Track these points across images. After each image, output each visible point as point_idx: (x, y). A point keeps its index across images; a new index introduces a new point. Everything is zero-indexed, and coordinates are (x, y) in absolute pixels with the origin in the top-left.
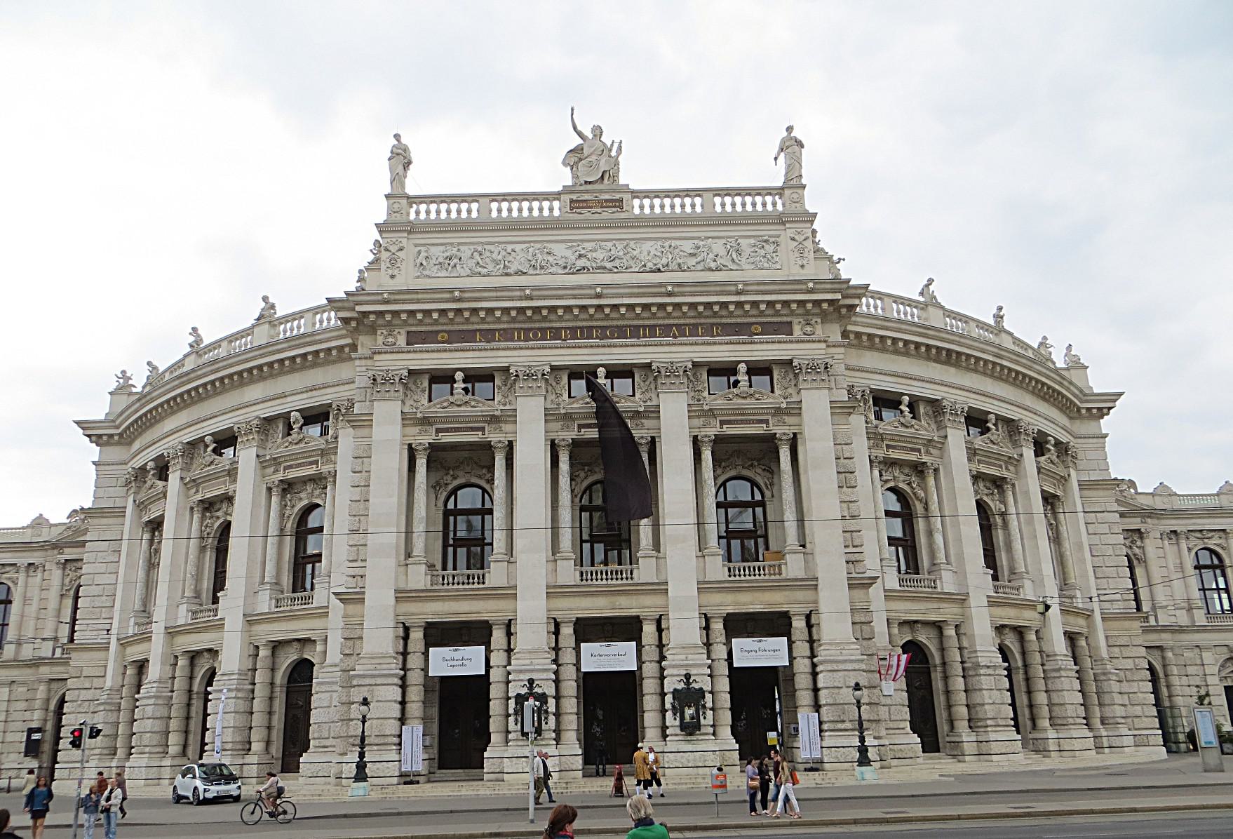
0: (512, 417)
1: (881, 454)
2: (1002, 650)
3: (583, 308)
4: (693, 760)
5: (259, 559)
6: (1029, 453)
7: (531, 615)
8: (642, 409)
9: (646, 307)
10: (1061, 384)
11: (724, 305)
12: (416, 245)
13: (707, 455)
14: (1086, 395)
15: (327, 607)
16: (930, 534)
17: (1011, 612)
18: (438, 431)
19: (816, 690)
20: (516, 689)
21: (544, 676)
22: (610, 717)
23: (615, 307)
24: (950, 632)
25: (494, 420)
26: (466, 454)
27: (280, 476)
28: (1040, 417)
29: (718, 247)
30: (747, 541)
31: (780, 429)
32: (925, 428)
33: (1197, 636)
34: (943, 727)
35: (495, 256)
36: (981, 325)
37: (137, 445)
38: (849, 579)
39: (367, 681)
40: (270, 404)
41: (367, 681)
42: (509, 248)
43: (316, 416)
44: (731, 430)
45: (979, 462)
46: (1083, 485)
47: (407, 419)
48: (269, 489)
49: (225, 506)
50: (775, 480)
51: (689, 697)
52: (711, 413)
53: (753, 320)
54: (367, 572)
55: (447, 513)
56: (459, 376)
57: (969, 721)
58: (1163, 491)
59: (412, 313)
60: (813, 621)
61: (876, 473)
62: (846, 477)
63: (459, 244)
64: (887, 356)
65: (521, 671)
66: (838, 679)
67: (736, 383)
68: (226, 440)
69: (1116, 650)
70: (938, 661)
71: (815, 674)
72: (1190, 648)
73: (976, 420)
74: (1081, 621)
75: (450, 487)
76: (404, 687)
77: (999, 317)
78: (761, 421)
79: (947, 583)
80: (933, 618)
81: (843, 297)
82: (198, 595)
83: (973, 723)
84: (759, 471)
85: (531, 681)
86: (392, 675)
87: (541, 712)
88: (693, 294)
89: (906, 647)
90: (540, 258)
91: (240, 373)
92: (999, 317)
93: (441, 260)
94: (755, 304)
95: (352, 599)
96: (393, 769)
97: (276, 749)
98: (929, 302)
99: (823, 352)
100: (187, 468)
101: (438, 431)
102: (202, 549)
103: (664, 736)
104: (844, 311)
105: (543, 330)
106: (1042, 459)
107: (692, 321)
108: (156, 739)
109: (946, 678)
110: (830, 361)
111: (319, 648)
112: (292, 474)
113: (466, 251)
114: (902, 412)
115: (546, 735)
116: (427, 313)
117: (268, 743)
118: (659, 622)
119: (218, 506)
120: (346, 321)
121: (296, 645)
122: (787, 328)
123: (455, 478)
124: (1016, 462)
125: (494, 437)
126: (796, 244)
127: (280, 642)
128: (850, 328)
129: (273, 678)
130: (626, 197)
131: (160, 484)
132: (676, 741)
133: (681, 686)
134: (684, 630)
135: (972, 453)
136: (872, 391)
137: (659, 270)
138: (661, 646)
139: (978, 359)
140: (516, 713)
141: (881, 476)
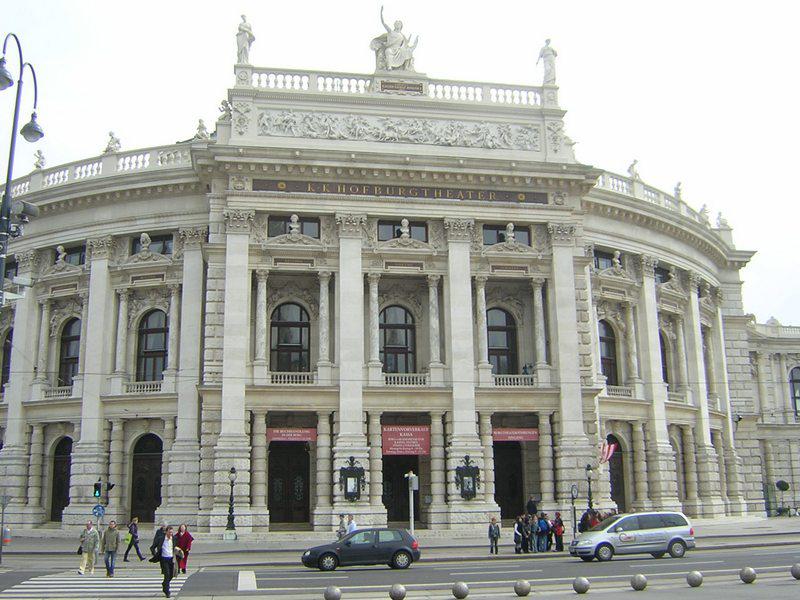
0: (336, 254)
1: (598, 294)
2: (672, 442)
3: (394, 171)
4: (466, 521)
5: (110, 351)
6: (694, 296)
7: (352, 407)
9: (442, 175)
10: (715, 242)
11: (500, 178)
12: (259, 108)
14: (732, 252)
15: (177, 394)
16: (628, 355)
17: (679, 415)
18: (276, 261)
19: (555, 469)
20: (339, 464)
21: (362, 455)
22: (403, 482)
23: (419, 173)
24: (639, 428)
25: (321, 255)
26: (290, 278)
27: (129, 285)
28: (704, 270)
29: (494, 131)
30: (508, 359)
32: (627, 277)
33: (789, 432)
34: (629, 497)
35: (322, 122)
36: (667, 197)
38: (583, 390)
39: (227, 455)
40: (120, 224)
41: (227, 455)
42: (333, 116)
43: (162, 238)
44: (499, 274)
45: (663, 302)
46: (725, 320)
47: (254, 251)
48: (118, 296)
49: (71, 305)
50: (527, 311)
51: (469, 471)
53: (519, 190)
54: (224, 370)
55: (273, 325)
56: (295, 218)
57: (648, 492)
58: (773, 324)
59: (259, 165)
60: (555, 419)
61: (595, 308)
62: (582, 317)
63: (294, 111)
64: (604, 219)
65: (344, 451)
66: (573, 462)
67: (501, 239)
68: (77, 250)
69: (739, 442)
70: (628, 448)
71: (554, 458)
72: (780, 441)
73: (663, 272)
74: (719, 421)
75: (277, 304)
76: (252, 459)
77: (677, 189)
78: (522, 268)
79: (639, 393)
80: (628, 418)
81: (587, 178)
82: (47, 373)
83: (651, 494)
84: (514, 304)
85: (352, 459)
86: (245, 451)
87: (360, 483)
88: (477, 167)
89: (612, 439)
90: (359, 126)
91: (93, 197)
92: (677, 189)
93: (279, 122)
94: (523, 179)
96: (249, 520)
97: (127, 503)
100: (36, 271)
101: (276, 261)
102: (50, 339)
103: (446, 498)
105: (361, 186)
106: (703, 299)
107: (474, 188)
108: (15, 492)
109: (633, 462)
111: (168, 426)
112: (139, 284)
113: (298, 119)
114: (613, 264)
115: (363, 498)
116: (272, 166)
117: (121, 498)
118: (444, 417)
119: (64, 304)
120: (203, 167)
121: (145, 423)
122: (541, 198)
123: (281, 297)
124: (686, 303)
125: (320, 268)
126: (551, 133)
127: (128, 420)
128: (586, 198)
129: (124, 447)
130: (424, 83)
132: (457, 504)
133: (463, 465)
134: (464, 423)
135: (659, 295)
136: (596, 246)
137: (449, 145)
138: (445, 435)
139: (667, 225)
140: (341, 482)
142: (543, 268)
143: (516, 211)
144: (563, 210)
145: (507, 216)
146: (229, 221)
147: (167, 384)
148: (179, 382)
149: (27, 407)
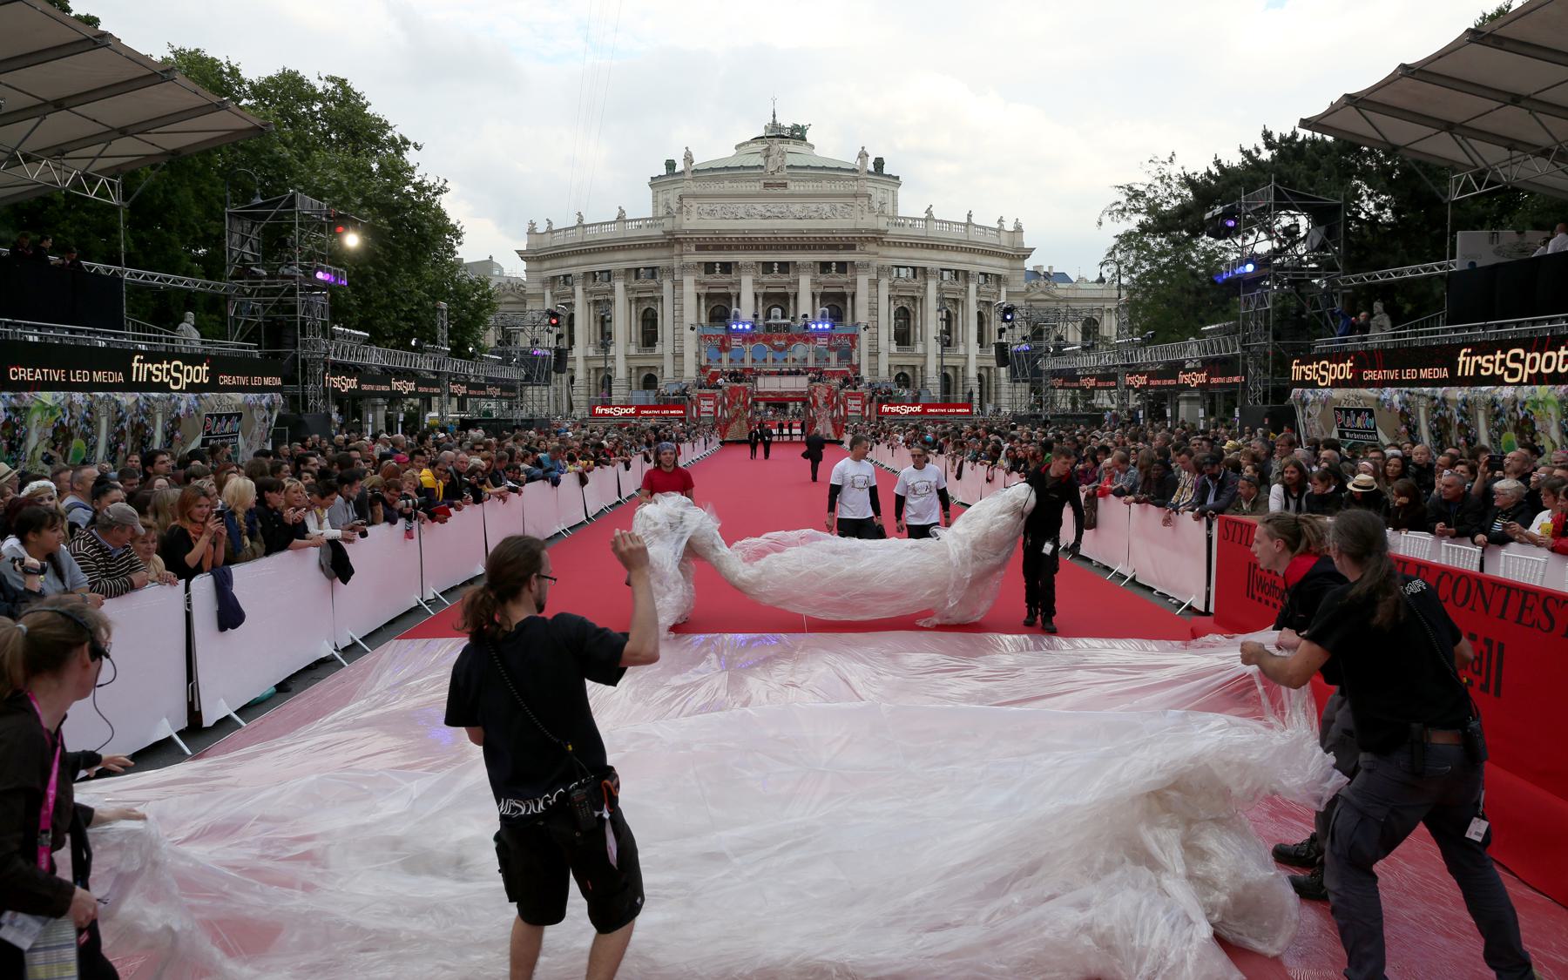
0: (739, 283)
29: (827, 208)
31: (847, 290)
37: (547, 264)
43: (653, 272)
47: (697, 283)
77: (969, 216)
79: (919, 349)
92: (969, 216)
95: (678, 356)
98: (929, 217)
125: (732, 291)
131: (569, 289)
146: (685, 268)
147: (658, 349)
148: (664, 347)
149: (587, 359)
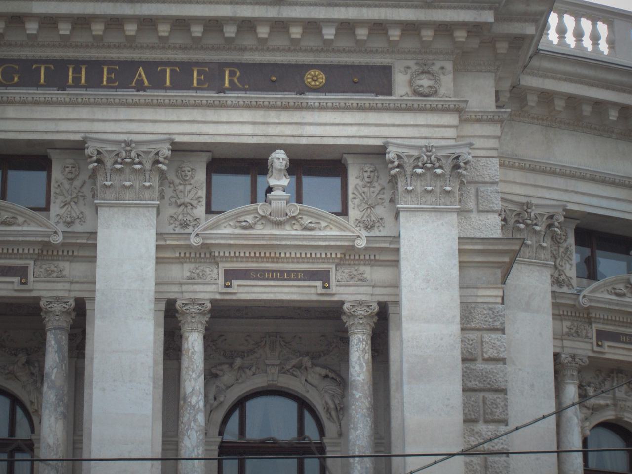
1: (583, 348)
8: (58, 239)
13: (194, 343)
52: (206, 254)
61: (571, 391)
94: (313, 26)
99: (451, 133)
104: (502, 47)
107: (180, 56)
110: (466, 154)
136: (570, 215)
141: (583, 396)
142: (379, 274)
143: (297, 116)
144: (433, 110)
145: (271, 130)
